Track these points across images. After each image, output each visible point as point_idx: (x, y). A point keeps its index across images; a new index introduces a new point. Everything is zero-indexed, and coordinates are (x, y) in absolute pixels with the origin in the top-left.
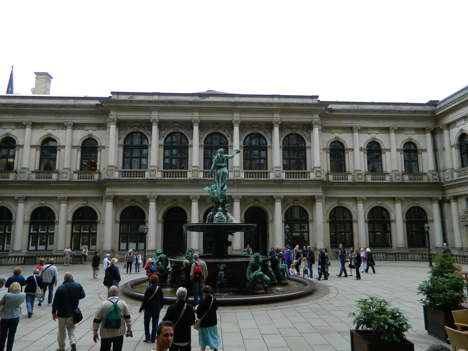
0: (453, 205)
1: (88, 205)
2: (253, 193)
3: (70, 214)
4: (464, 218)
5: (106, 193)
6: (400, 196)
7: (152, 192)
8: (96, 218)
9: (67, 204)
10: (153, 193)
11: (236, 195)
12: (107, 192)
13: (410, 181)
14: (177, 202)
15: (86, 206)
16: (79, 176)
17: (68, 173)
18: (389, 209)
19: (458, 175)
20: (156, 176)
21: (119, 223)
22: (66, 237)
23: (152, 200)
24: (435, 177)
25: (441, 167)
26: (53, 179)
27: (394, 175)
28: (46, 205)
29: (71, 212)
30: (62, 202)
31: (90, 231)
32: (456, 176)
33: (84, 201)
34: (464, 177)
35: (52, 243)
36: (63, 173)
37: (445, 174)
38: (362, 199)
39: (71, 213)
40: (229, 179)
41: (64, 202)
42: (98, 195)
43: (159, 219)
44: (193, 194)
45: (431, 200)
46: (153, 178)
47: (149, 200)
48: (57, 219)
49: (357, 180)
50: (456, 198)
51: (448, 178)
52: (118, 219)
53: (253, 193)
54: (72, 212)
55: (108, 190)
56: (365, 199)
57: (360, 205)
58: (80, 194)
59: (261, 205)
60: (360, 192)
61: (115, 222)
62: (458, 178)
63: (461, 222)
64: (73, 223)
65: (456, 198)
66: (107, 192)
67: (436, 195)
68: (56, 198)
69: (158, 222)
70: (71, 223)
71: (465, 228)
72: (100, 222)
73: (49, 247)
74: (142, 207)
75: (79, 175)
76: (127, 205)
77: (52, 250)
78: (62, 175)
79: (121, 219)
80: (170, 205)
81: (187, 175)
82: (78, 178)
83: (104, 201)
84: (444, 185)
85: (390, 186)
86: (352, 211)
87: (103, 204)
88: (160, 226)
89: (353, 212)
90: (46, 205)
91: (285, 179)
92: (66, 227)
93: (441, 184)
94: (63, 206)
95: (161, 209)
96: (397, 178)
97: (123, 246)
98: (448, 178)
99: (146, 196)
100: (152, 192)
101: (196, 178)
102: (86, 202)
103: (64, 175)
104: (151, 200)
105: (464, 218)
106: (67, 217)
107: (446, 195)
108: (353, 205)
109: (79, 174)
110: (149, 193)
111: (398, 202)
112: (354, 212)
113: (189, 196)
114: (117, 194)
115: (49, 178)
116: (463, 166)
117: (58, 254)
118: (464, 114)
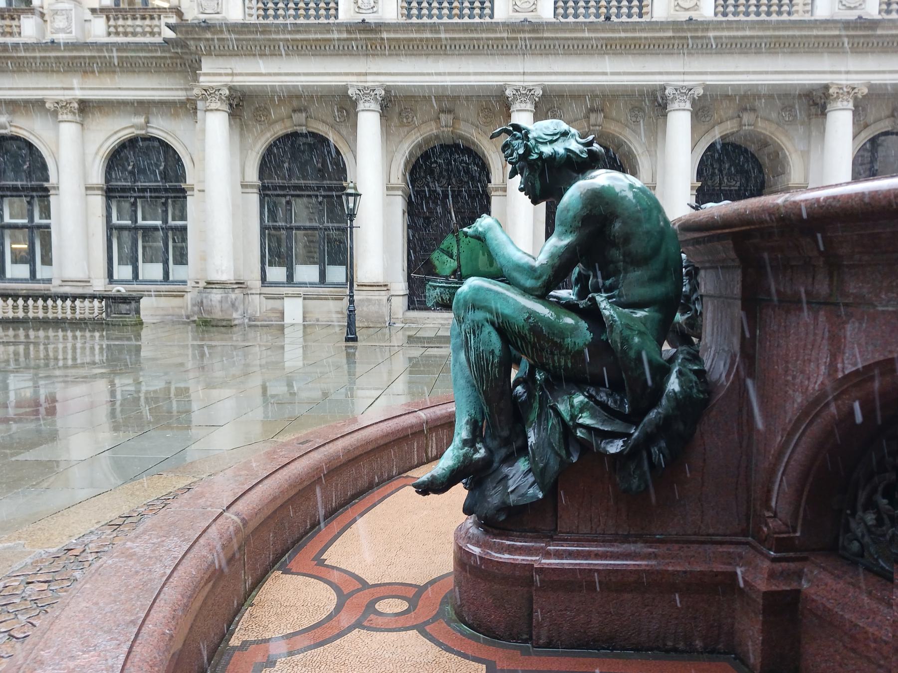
1: (150, 130)
2: (748, 73)
3: (94, 158)
5: (202, 79)
7: (366, 74)
8: (182, 177)
9: (82, 125)
10: (369, 78)
11: (681, 83)
12: (205, 74)
14: (456, 119)
15: (143, 132)
16: (109, 27)
17: (73, 12)
20: (380, 10)
21: (256, 190)
22: (87, 235)
23: (367, 104)
26: (25, 37)
28: (13, 129)
29: (97, 153)
30: (60, 117)
31: (165, 221)
33: (136, 113)
35: (47, 260)
36: (56, 12)
39: (98, 158)
40: (653, 20)
41: (70, 117)
42: (180, 95)
43: (392, 181)
44: (517, 81)
46: (371, 18)
47: (355, 103)
48: (53, 179)
52: (253, 176)
53: (748, 73)
54: (101, 154)
55: (207, 65)
58: (120, 89)
59: (765, 128)
61: (243, 186)
64: (110, 193)
66: (205, 74)
68: (39, 104)
69: (388, 189)
70: (100, 192)
72: (193, 189)
73: (42, 272)
74: (332, 137)
75: (112, 22)
76: (280, 130)
77: (49, 281)
78: (51, 22)
79: (261, 177)
80: (430, 130)
81: (492, 9)
82: (109, 34)
83: (200, 114)
87: (198, 126)
88: (399, 204)
90: (13, 129)
91: (879, 17)
92: (86, 207)
94: (68, 130)
95: (401, 141)
97: (277, 273)
99: (346, 88)
100: (366, 74)
101: (530, 17)
102: (141, 120)
103: (60, 22)
104: (361, 106)
106: (85, 175)
109: (108, 19)
110: (354, 78)
113: (502, 89)
114: (239, 81)
115: (11, 34)
117: (67, 290)
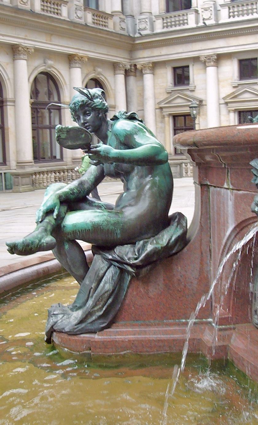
0: (148, 78)
6: (81, 53)
13: (93, 26)
18: (62, 79)
19: (165, 25)
24: (124, 25)
25: (128, 10)
27: (75, 7)
32: (159, 27)
34: (178, 28)
37: (138, 21)
38: (26, 50)
45: (115, 66)
49: (21, 6)
50: (155, 66)
51: (145, 29)
56: (33, 50)
57: (22, 64)
60: (22, 34)
62: (165, 30)
63: (157, 110)
65: (155, 66)
67: (122, 60)
71: (167, 119)
84: (138, 42)
85: (72, 28)
86: (6, 78)
89: (8, 81)
93: (134, 39)
96: (79, 15)
98: (145, 29)
107: (136, 61)
108: (7, 64)
111: (77, 65)
112: (9, 79)
116: (168, 11)
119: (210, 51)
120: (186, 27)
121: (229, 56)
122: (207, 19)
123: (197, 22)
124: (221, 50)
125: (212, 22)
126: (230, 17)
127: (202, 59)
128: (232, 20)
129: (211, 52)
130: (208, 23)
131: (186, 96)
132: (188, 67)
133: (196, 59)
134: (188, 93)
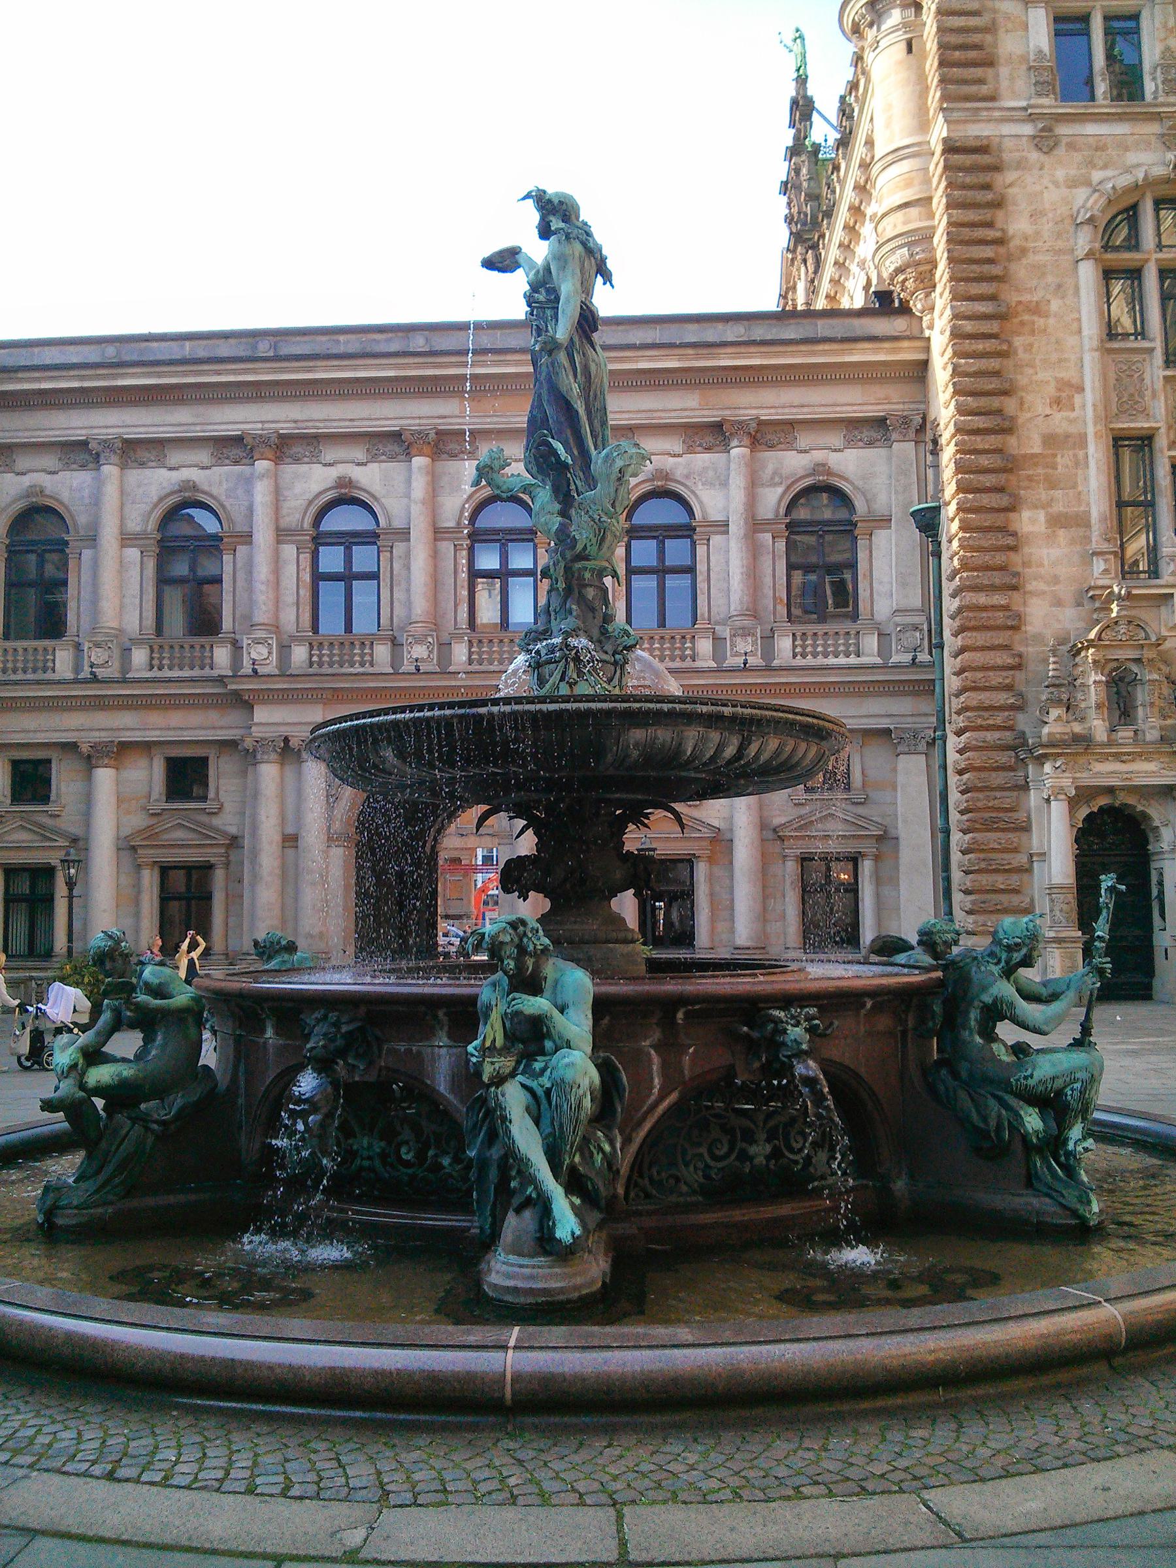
4: (800, 828)
105: (800, 828)
118: (79, 435)
119: (103, 734)
120: (49, 676)
121: (147, 747)
122: (98, 666)
123: (77, 668)
124: (128, 733)
125: (112, 671)
126: (152, 667)
127: (85, 748)
128: (155, 673)
129: (104, 736)
130: (101, 673)
131: (36, 824)
132: (49, 761)
133: (70, 747)
134: (45, 820)
